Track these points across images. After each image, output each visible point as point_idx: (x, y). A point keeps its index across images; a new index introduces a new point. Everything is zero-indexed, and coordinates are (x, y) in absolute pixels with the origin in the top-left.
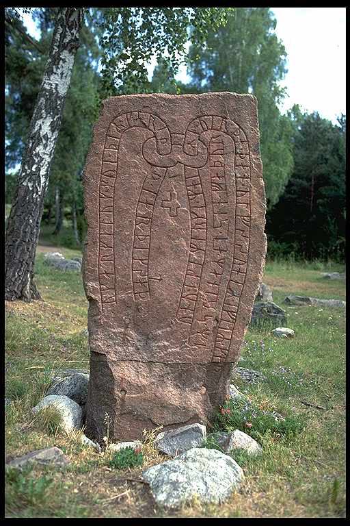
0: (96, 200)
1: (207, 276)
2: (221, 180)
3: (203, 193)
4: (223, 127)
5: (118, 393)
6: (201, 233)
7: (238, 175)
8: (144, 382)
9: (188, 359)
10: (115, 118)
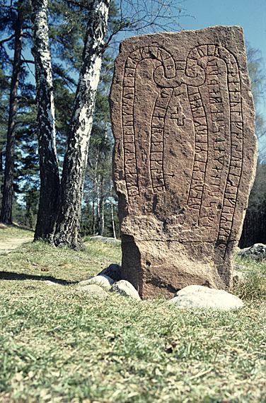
1: (210, 171)
2: (217, 95)
4: (217, 52)
6: (204, 137)
7: (231, 90)
8: (164, 255)
9: (198, 237)
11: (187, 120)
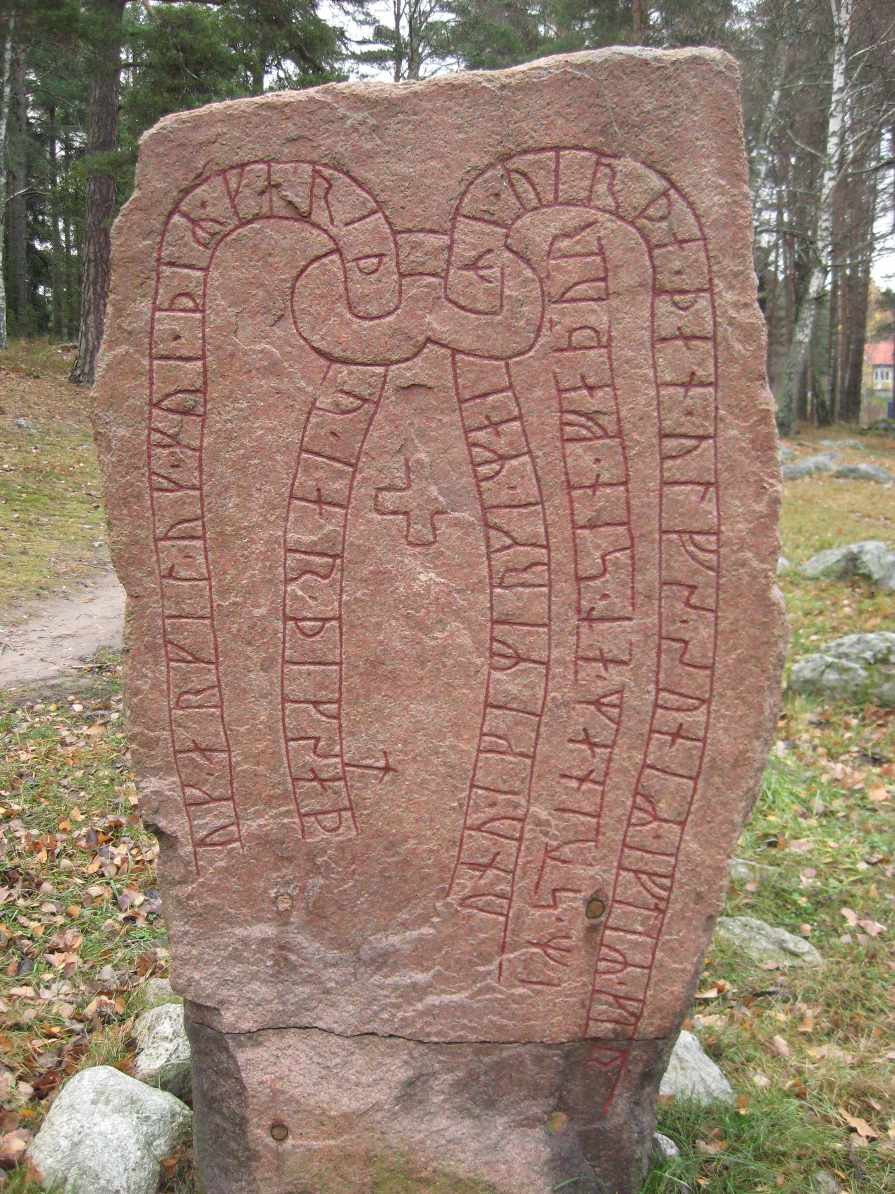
0: (139, 497)
2: (600, 400)
3: (529, 452)
4: (602, 188)
10: (186, 192)
11: (457, 523)
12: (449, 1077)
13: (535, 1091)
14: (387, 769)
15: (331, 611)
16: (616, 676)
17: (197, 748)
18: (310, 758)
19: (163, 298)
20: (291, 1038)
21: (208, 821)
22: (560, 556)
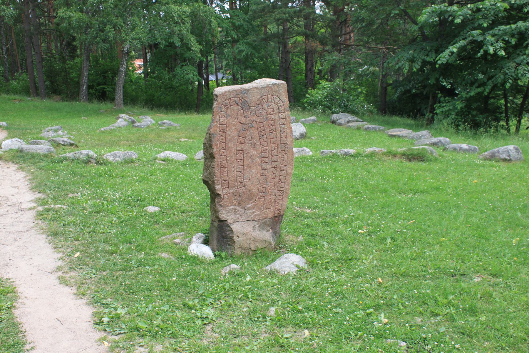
5: (235, 238)
12: (258, 225)
13: (269, 226)
14: (249, 180)
15: (242, 158)
16: (276, 163)
17: (224, 181)
18: (239, 180)
19: (221, 117)
20: (237, 223)
21: (225, 191)
22: (269, 148)
